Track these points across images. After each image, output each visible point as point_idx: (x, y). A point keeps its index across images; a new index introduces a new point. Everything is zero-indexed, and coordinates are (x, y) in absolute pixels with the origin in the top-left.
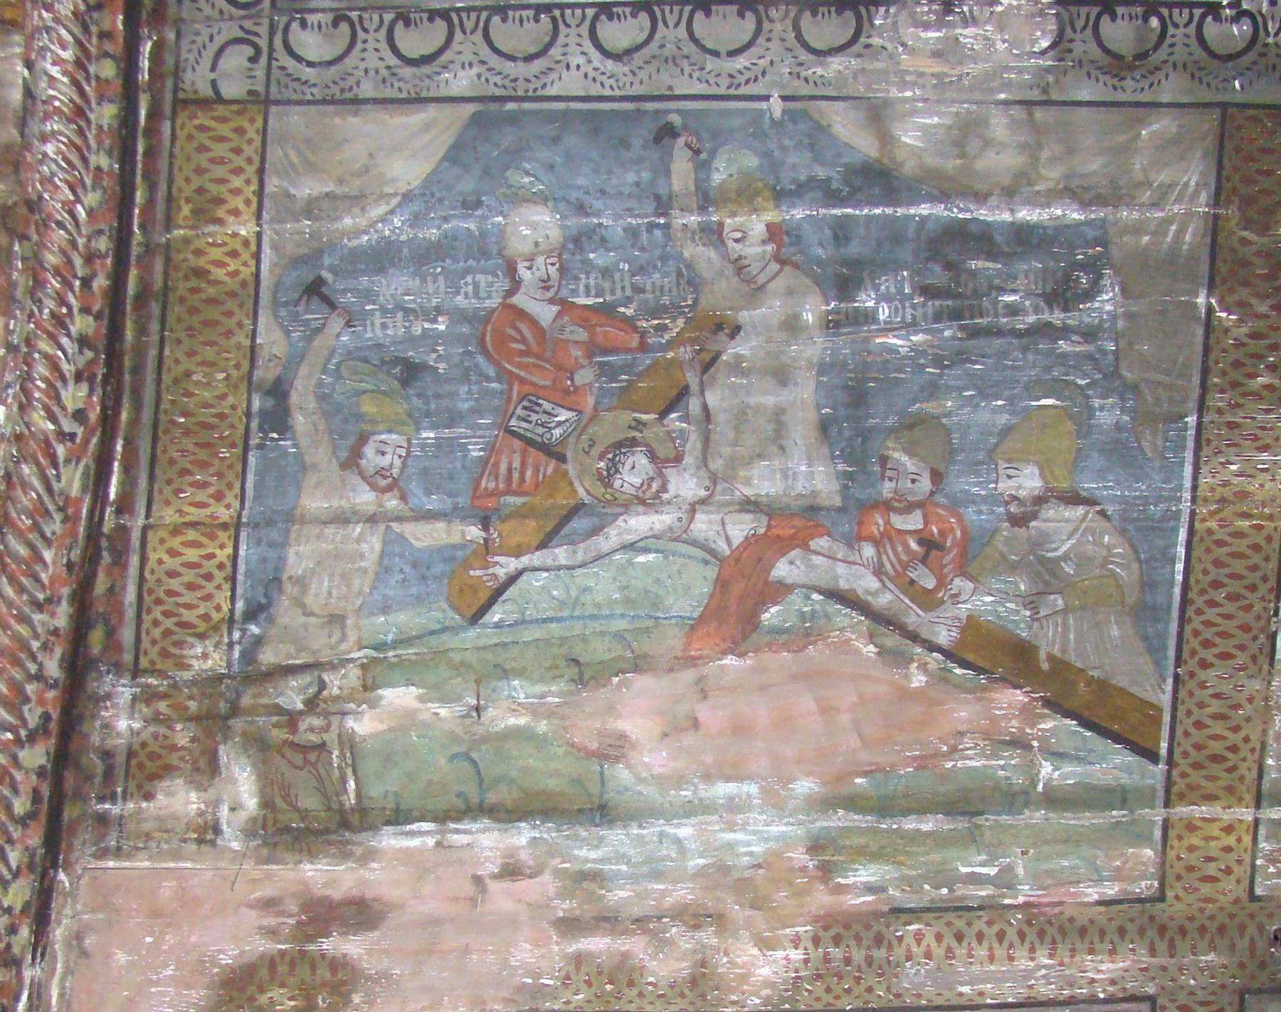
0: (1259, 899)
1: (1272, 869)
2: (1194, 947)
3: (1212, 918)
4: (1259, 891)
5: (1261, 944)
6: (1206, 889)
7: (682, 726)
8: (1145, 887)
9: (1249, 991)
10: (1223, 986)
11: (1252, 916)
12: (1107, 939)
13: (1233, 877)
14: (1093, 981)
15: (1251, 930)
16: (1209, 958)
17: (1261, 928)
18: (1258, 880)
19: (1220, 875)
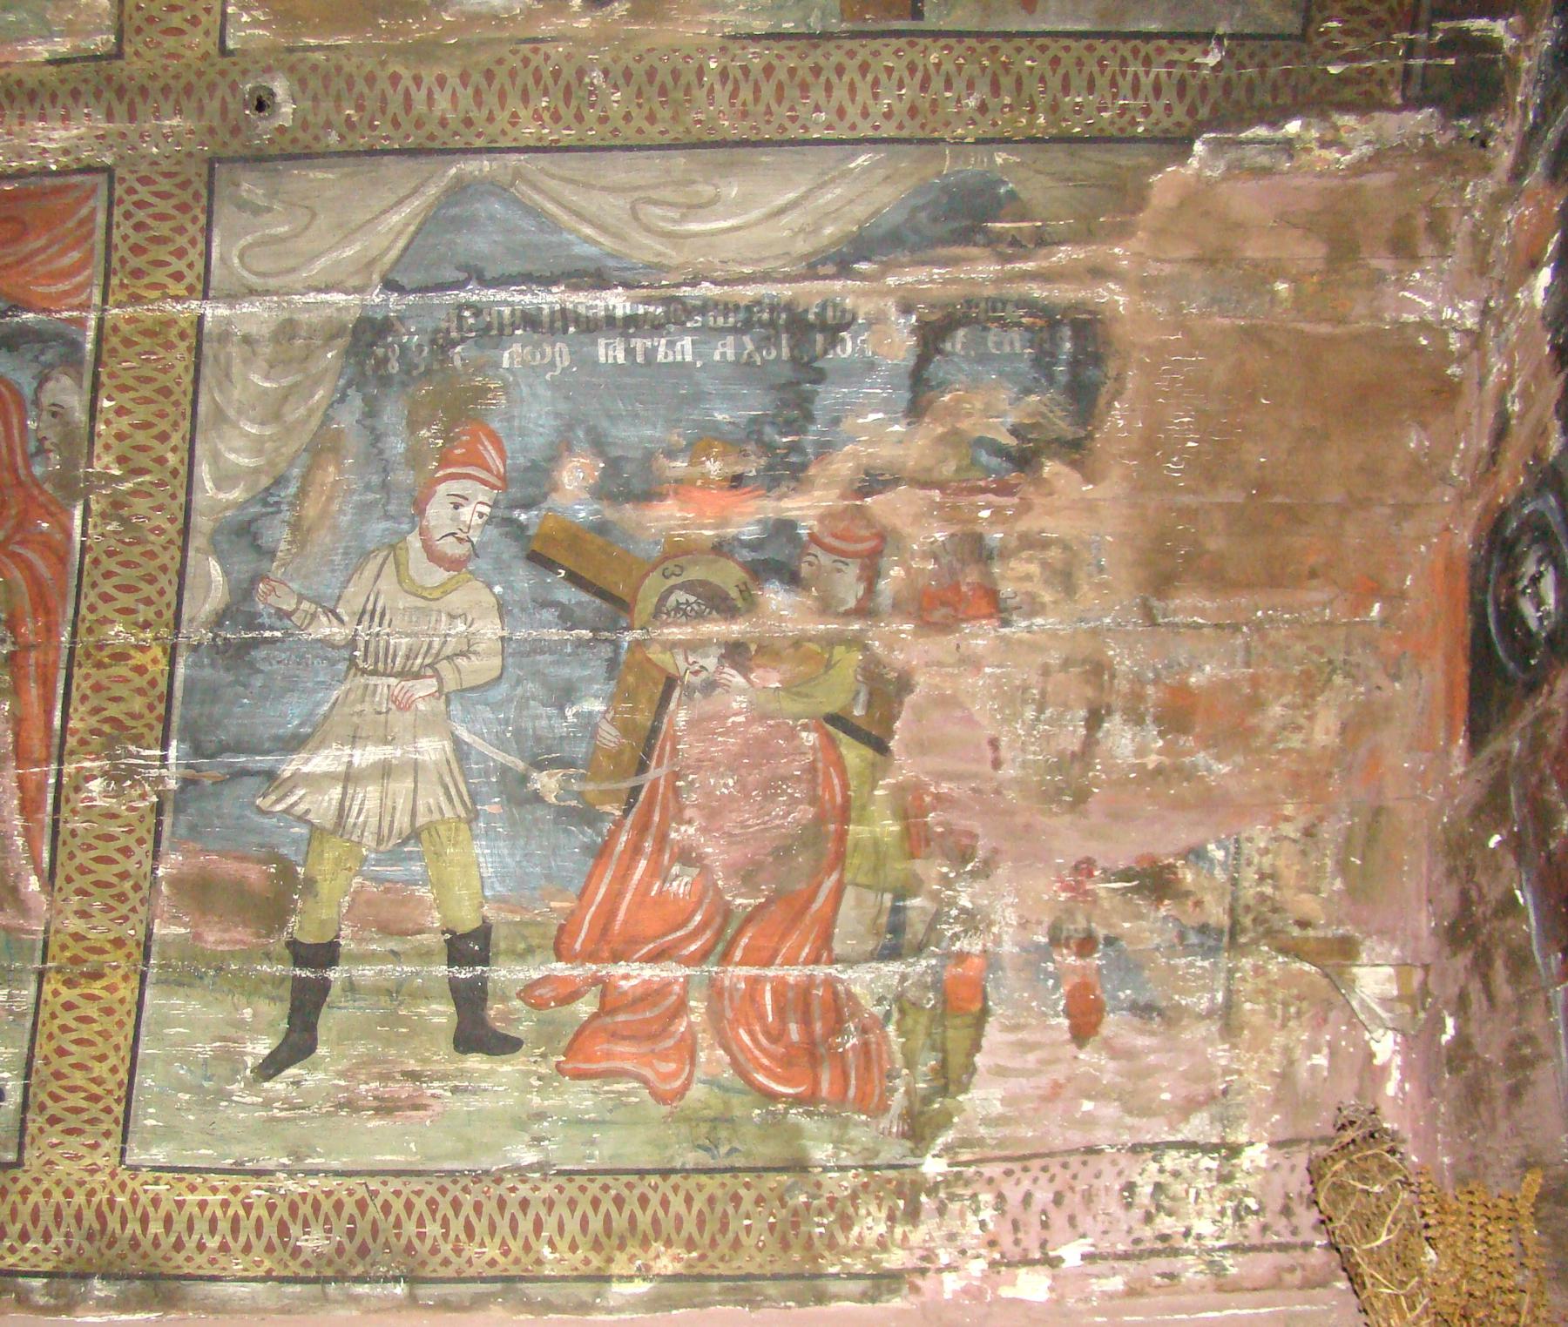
0: (232, 53)
1: (245, 18)
2: (158, 109)
3: (177, 77)
4: (231, 44)
5: (233, 105)
6: (170, 43)
8: (102, 41)
9: (220, 160)
10: (190, 155)
11: (223, 73)
12: (59, 103)
13: (201, 29)
14: (45, 150)
15: (223, 90)
16: (174, 122)
17: (234, 87)
18: (230, 30)
19: (185, 26)
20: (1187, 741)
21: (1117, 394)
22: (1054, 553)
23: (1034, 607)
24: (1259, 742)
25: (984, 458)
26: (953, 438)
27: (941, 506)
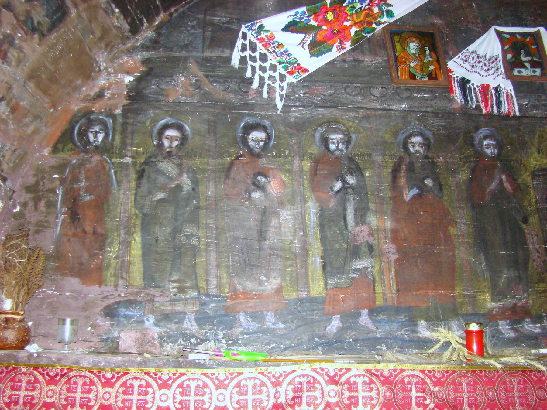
20: (11, 116)
21: (57, 32)
22: (22, 55)
23: (9, 65)
24: (21, 125)
25: (29, 23)
26: (28, 12)
27: (14, 25)
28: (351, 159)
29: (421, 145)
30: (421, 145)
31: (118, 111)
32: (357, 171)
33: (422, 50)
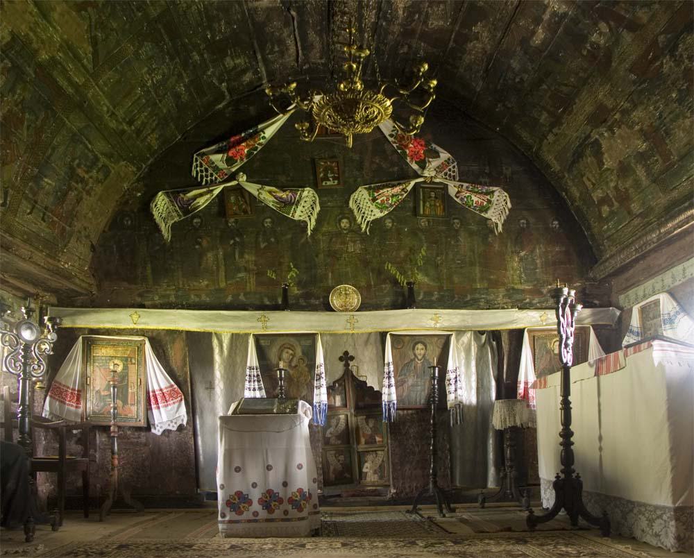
7: (62, 15)
8: (80, 84)
28: (238, 230)
29: (270, 223)
30: (270, 223)
31: (135, 210)
32: (241, 235)
33: (237, 199)
